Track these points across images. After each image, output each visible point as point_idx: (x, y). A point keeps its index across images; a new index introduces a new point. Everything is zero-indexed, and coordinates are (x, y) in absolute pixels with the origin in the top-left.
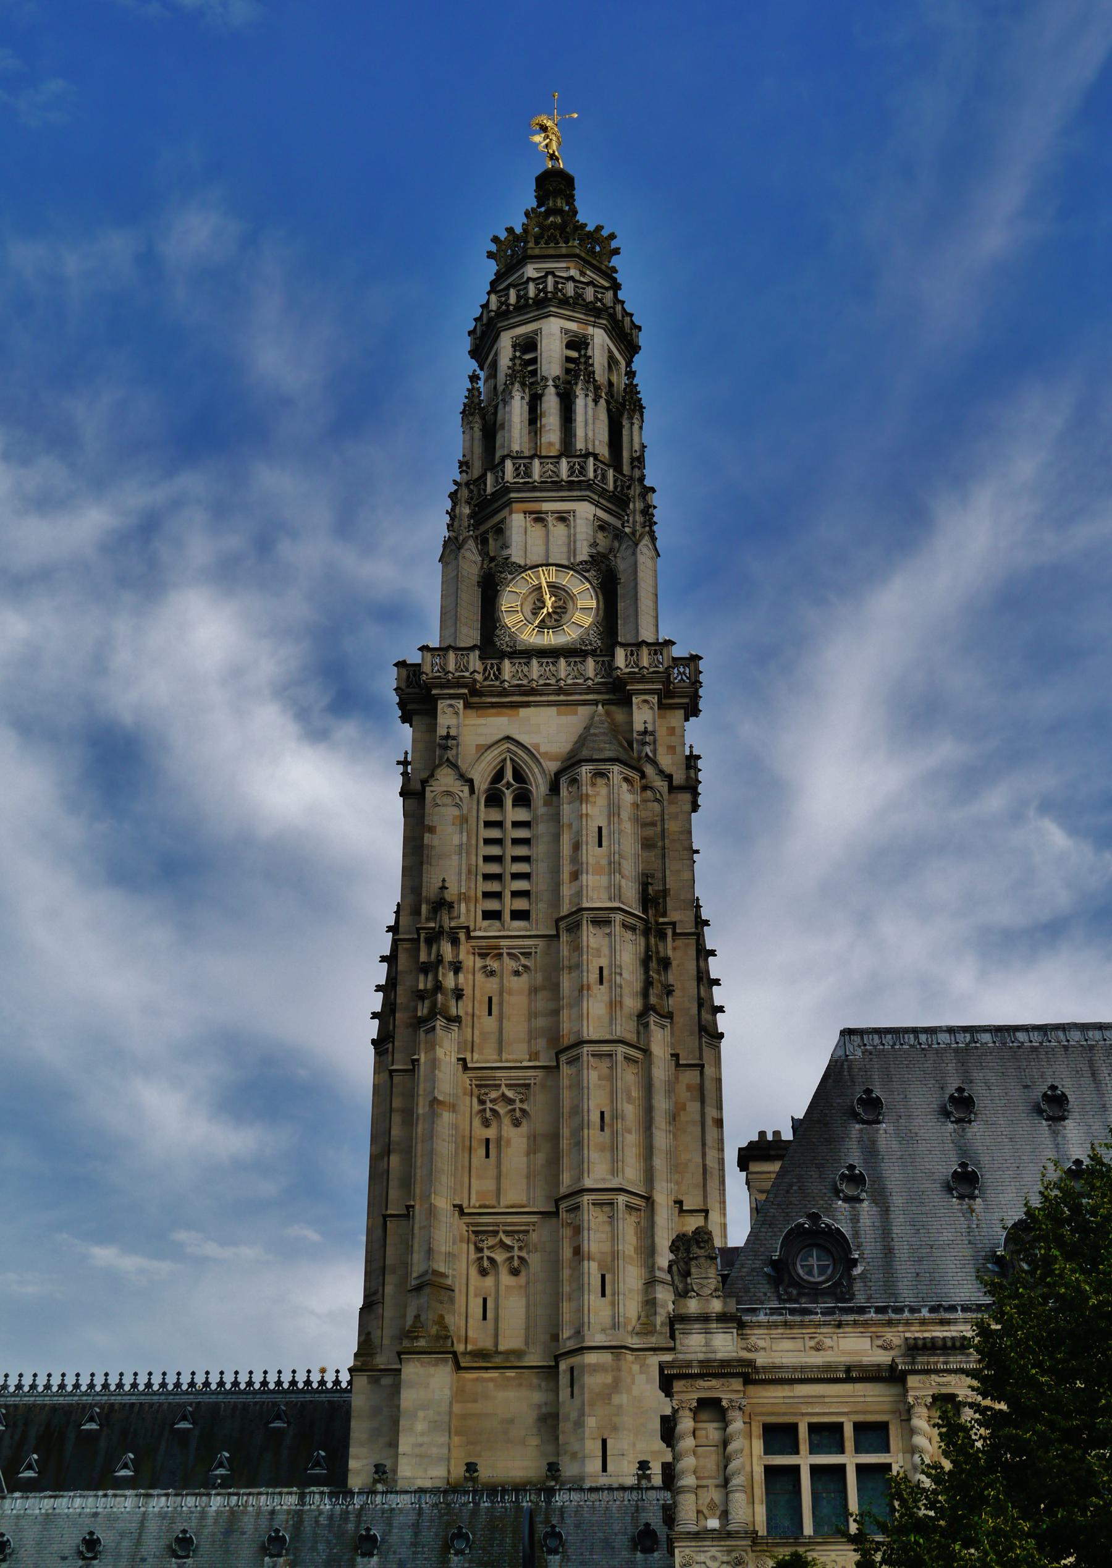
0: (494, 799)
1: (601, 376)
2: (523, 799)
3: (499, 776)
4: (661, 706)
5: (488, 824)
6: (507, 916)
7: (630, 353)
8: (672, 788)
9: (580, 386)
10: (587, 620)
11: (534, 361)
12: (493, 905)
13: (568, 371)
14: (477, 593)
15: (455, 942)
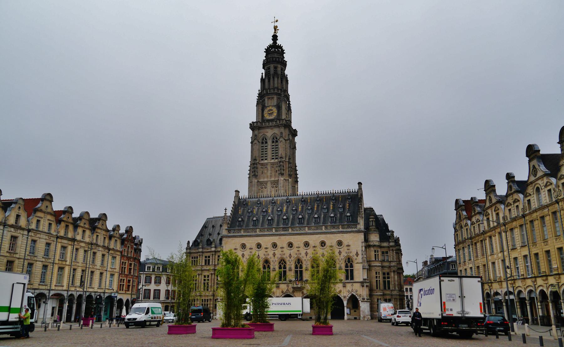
0: (263, 143)
1: (279, 73)
2: (266, 143)
3: (263, 140)
4: (284, 127)
5: (262, 147)
6: (264, 159)
7: (284, 67)
8: (285, 140)
9: (275, 76)
10: (275, 114)
11: (269, 71)
12: (262, 158)
13: (274, 72)
14: (261, 111)
15: (257, 164)
